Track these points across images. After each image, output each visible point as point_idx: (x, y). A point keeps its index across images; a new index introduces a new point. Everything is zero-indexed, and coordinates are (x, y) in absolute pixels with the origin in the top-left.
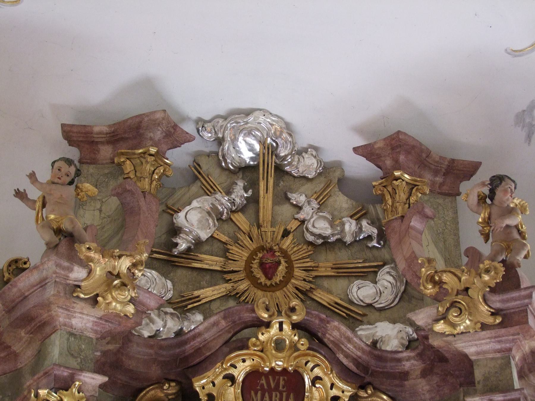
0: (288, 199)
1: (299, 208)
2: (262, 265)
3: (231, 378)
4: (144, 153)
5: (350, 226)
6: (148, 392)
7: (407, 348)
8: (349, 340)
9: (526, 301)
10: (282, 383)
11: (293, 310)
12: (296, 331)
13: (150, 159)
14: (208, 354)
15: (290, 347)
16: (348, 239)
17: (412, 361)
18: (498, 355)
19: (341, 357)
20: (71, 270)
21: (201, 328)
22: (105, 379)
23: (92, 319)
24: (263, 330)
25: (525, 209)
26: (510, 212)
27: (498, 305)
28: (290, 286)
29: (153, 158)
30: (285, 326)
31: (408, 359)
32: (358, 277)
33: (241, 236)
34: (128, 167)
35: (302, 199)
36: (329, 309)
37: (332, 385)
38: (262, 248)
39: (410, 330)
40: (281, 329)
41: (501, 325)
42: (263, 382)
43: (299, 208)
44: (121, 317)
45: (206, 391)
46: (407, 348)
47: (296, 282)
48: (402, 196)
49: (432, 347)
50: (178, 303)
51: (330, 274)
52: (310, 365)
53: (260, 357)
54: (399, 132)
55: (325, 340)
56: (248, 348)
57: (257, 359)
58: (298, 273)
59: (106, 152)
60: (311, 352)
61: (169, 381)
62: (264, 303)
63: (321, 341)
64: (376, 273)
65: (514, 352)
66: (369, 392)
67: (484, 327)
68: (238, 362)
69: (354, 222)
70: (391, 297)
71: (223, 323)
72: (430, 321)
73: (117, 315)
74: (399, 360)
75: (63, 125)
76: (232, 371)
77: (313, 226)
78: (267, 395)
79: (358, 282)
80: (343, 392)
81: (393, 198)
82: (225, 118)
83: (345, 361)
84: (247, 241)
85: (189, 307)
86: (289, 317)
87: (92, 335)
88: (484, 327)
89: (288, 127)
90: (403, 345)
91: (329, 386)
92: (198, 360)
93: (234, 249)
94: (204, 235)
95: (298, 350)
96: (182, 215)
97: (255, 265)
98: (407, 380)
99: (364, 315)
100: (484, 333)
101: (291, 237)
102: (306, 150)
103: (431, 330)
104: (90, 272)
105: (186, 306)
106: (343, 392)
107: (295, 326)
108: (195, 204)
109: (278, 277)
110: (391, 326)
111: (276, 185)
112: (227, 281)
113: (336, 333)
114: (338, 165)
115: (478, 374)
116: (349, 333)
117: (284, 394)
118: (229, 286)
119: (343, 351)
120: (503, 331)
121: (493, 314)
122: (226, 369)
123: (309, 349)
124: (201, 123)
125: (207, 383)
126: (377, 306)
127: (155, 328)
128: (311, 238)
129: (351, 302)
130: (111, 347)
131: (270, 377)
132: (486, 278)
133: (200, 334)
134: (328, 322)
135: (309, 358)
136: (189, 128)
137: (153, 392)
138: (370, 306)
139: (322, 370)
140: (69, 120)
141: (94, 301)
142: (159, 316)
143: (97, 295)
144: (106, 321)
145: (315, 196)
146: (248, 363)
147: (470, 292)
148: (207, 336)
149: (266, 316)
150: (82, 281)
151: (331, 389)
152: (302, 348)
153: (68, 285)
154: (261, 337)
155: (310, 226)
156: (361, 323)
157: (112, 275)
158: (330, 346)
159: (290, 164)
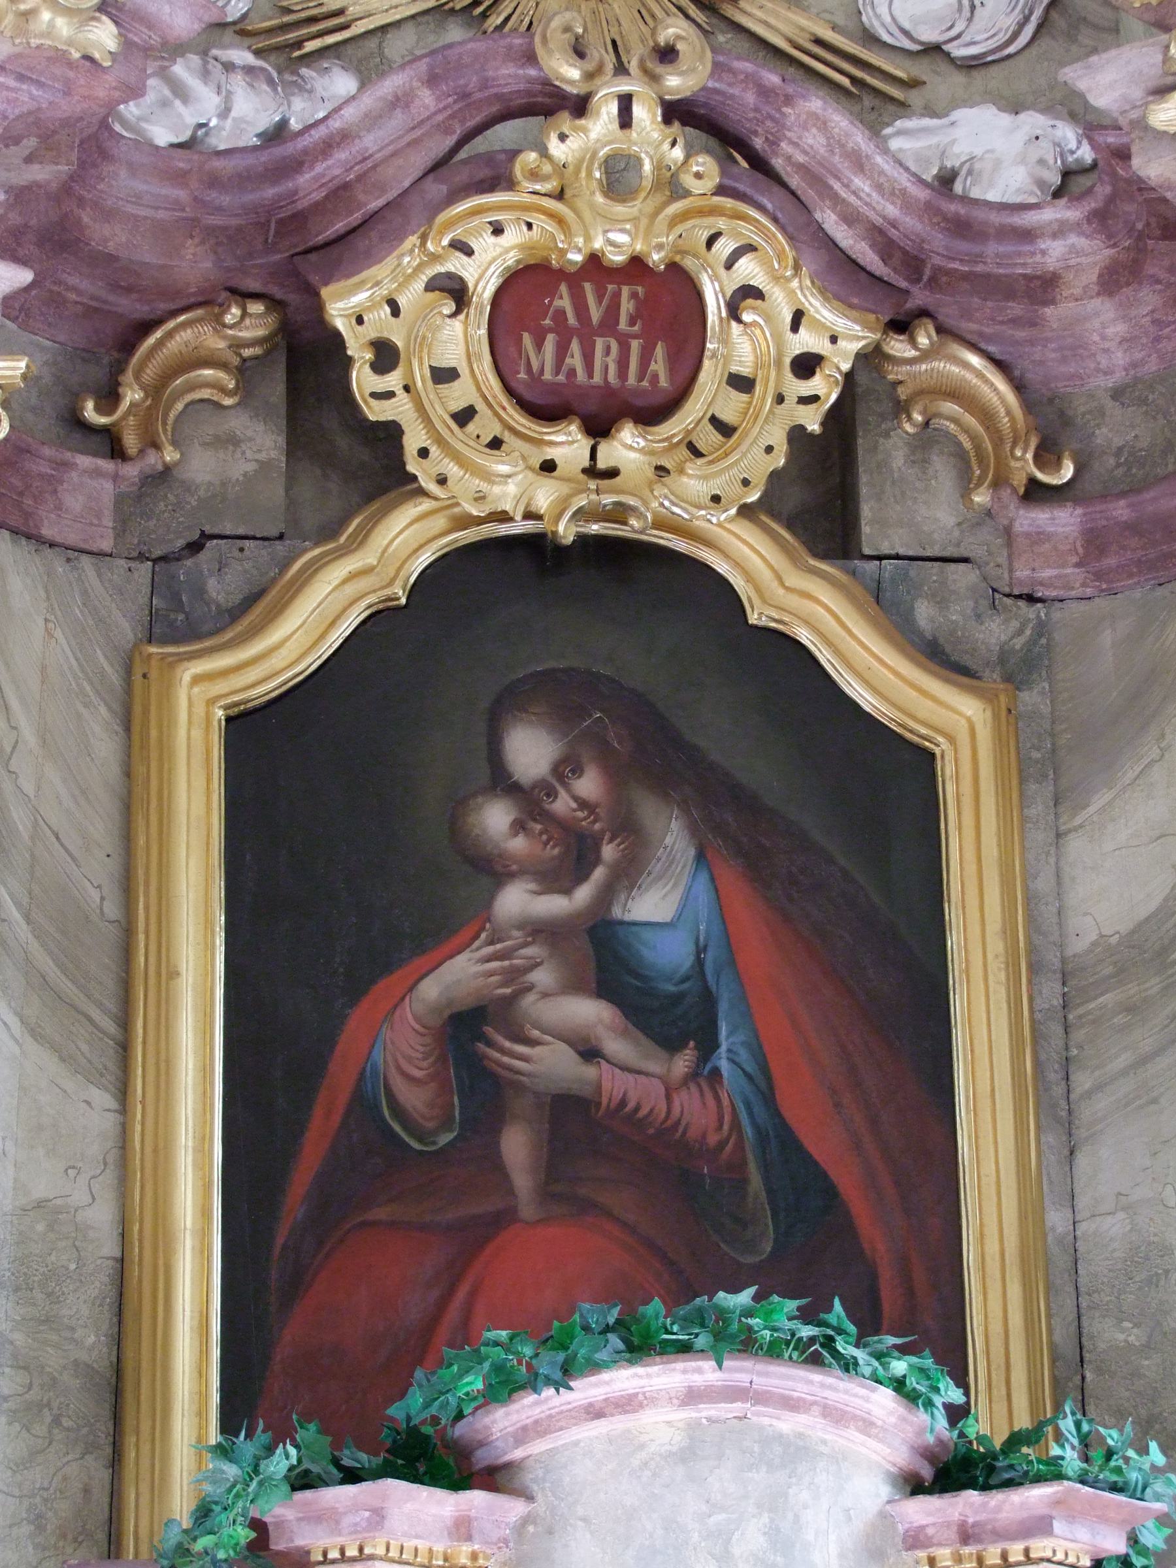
6: (170, 335)
7: (1057, 194)
8: (859, 163)
10: (627, 306)
11: (667, 54)
12: (677, 125)
14: (375, 204)
15: (657, 186)
17: (1073, 239)
19: (829, 220)
21: (350, 114)
22: (25, 276)
24: (565, 121)
31: (1060, 230)
36: (792, 60)
39: (1068, 134)
40: (625, 119)
42: (564, 302)
44: (70, 64)
45: (370, 331)
46: (1057, 194)
49: (1140, 186)
50: (270, 31)
52: (725, 247)
53: (551, 215)
55: (778, 163)
56: (510, 184)
57: (538, 220)
60: (728, 203)
62: (567, 29)
63: (759, 164)
66: (923, 341)
68: (478, 232)
70: (1009, 22)
71: (426, 99)
72: (1137, 93)
73: (59, 57)
74: (1027, 235)
76: (456, 264)
78: (575, 346)
80: (834, 339)
83: (844, 237)
85: (310, 46)
86: (653, 78)
90: (1041, 184)
91: (788, 318)
92: (340, 226)
98: (1053, 302)
99: (913, 84)
103: (1141, 124)
105: (299, 44)
106: (834, 339)
110: (1005, 119)
113: (814, 140)
116: (859, 139)
117: (635, 345)
119: (836, 201)
122: (435, 258)
123: (721, 190)
125: (373, 306)
126: (958, 51)
127: (189, 116)
129: (870, 39)
130: (39, 173)
131: (588, 287)
133: (344, 137)
134: (788, 100)
135: (721, 224)
137: (187, 335)
138: (934, 50)
139: (766, 264)
142: (205, 75)
144: (21, 78)
146: (513, 236)
148: (370, 142)
149: (574, 73)
151: (795, 327)
152: (697, 187)
158: (794, 181)
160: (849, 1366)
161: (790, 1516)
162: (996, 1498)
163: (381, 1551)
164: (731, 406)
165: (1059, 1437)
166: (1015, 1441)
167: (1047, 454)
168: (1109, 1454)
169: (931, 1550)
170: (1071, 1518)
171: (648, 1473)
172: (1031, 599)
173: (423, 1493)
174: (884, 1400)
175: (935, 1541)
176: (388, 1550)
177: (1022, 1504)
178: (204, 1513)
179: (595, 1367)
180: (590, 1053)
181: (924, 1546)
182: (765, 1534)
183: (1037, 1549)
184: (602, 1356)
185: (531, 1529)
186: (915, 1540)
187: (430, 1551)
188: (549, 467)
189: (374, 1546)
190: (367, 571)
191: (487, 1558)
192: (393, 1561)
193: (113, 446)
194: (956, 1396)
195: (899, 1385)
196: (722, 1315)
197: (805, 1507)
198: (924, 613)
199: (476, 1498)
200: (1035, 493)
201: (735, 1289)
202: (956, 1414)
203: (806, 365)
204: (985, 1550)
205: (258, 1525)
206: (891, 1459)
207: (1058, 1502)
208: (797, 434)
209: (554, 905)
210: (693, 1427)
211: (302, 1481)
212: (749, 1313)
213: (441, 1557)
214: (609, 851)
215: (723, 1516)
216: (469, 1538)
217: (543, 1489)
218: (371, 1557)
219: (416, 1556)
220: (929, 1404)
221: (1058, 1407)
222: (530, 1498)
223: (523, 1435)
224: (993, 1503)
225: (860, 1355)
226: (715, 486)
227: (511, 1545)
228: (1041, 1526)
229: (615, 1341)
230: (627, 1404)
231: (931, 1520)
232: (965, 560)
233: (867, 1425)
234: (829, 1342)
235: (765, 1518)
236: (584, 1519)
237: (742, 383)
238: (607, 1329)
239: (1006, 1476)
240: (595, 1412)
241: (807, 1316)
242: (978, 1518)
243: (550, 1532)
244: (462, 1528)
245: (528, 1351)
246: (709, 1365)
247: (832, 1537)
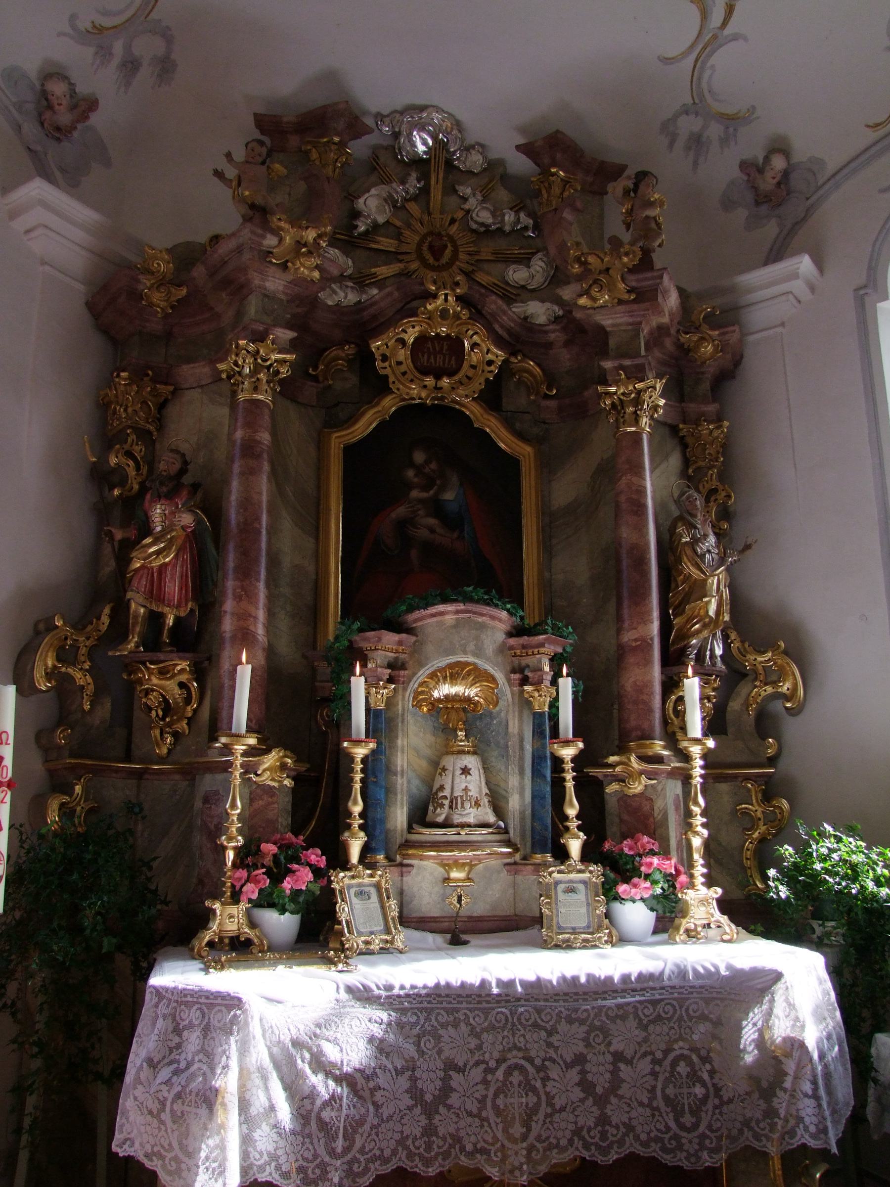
0: (456, 191)
1: (465, 199)
2: (431, 247)
3: (403, 342)
4: (328, 142)
5: (509, 217)
6: (331, 353)
7: (554, 322)
8: (505, 313)
9: (658, 281)
10: (445, 347)
11: (457, 284)
13: (334, 147)
14: (382, 320)
15: (454, 317)
16: (507, 228)
17: (557, 334)
18: (630, 327)
19: (497, 327)
20: (263, 237)
21: (377, 297)
22: (295, 334)
23: (283, 283)
24: (431, 301)
25: (663, 204)
26: (651, 204)
27: (634, 284)
28: (454, 267)
29: (336, 147)
30: (449, 298)
31: (554, 331)
32: (515, 262)
33: (413, 222)
34: (314, 155)
35: (469, 191)
37: (488, 351)
38: (431, 233)
39: (556, 308)
40: (446, 300)
41: (634, 301)
42: (430, 345)
43: (465, 199)
44: (308, 282)
45: (381, 352)
46: (554, 322)
47: (461, 265)
48: (556, 190)
49: (574, 319)
50: (357, 278)
51: (490, 258)
52: (470, 332)
53: (428, 324)
54: (557, 132)
55: (484, 312)
56: (417, 316)
57: (424, 325)
58: (462, 256)
59: (294, 141)
60: (471, 322)
61: (349, 343)
63: (479, 312)
64: (530, 259)
65: (643, 326)
67: (621, 302)
69: (513, 214)
70: (542, 280)
71: (396, 294)
72: (575, 296)
73: (305, 280)
74: (546, 332)
75: (255, 115)
76: (403, 335)
77: (477, 215)
78: (432, 357)
79: (513, 266)
81: (548, 192)
82: (402, 113)
84: (418, 226)
85: (367, 282)
86: (453, 290)
87: (282, 297)
88: (621, 302)
89: (458, 124)
90: (549, 320)
92: (374, 325)
93: (407, 233)
94: (381, 220)
95: (459, 318)
96: (361, 201)
97: (425, 247)
98: (551, 349)
100: (620, 307)
101: (457, 223)
102: (473, 147)
103: (576, 304)
104: (281, 240)
105: (364, 281)
107: (459, 299)
108: (373, 191)
109: (445, 259)
110: (540, 304)
111: (445, 178)
112: (401, 261)
113: (493, 306)
114: (500, 163)
115: (612, 342)
116: (505, 307)
118: (402, 266)
119: (498, 321)
120: (635, 306)
121: (628, 291)
122: (397, 334)
124: (380, 117)
126: (529, 287)
127: (336, 298)
128: (474, 226)
129: (507, 284)
130: (299, 310)
131: (436, 342)
132: (625, 260)
133: (375, 303)
134: (487, 296)
135: (470, 327)
136: (369, 122)
137: (335, 352)
138: (523, 287)
139: (480, 337)
140: (261, 110)
141: (284, 267)
142: (341, 288)
143: (287, 261)
144: (295, 285)
145: (480, 189)
146: (417, 329)
147: (611, 271)
148: (382, 304)
150: (274, 248)
152: (464, 317)
153: (261, 251)
154: (429, 307)
155: (474, 215)
156: (516, 301)
157: (300, 244)
158: (488, 317)
159: (458, 158)
160: (496, 606)
162: (532, 638)
164: (471, 373)
165: (547, 624)
166: (536, 625)
167: (550, 388)
168: (559, 628)
170: (549, 644)
172: (544, 423)
173: (391, 634)
174: (504, 614)
178: (337, 638)
179: (434, 605)
180: (432, 531)
184: (436, 602)
186: (511, 648)
188: (425, 387)
190: (379, 411)
193: (315, 379)
194: (522, 613)
195: (508, 610)
196: (465, 592)
198: (518, 425)
199: (404, 635)
200: (546, 397)
201: (469, 586)
202: (522, 618)
203: (490, 363)
205: (350, 641)
207: (546, 639)
208: (487, 380)
209: (424, 495)
210: (457, 619)
211: (361, 630)
212: (472, 592)
214: (438, 482)
220: (516, 615)
221: (546, 617)
223: (416, 621)
225: (499, 603)
226: (466, 392)
228: (542, 645)
229: (439, 598)
230: (442, 614)
232: (528, 413)
233: (500, 620)
234: (491, 600)
237: (474, 367)
238: (436, 596)
240: (433, 615)
241: (486, 593)
244: (400, 643)
245: (417, 600)
246: (462, 604)
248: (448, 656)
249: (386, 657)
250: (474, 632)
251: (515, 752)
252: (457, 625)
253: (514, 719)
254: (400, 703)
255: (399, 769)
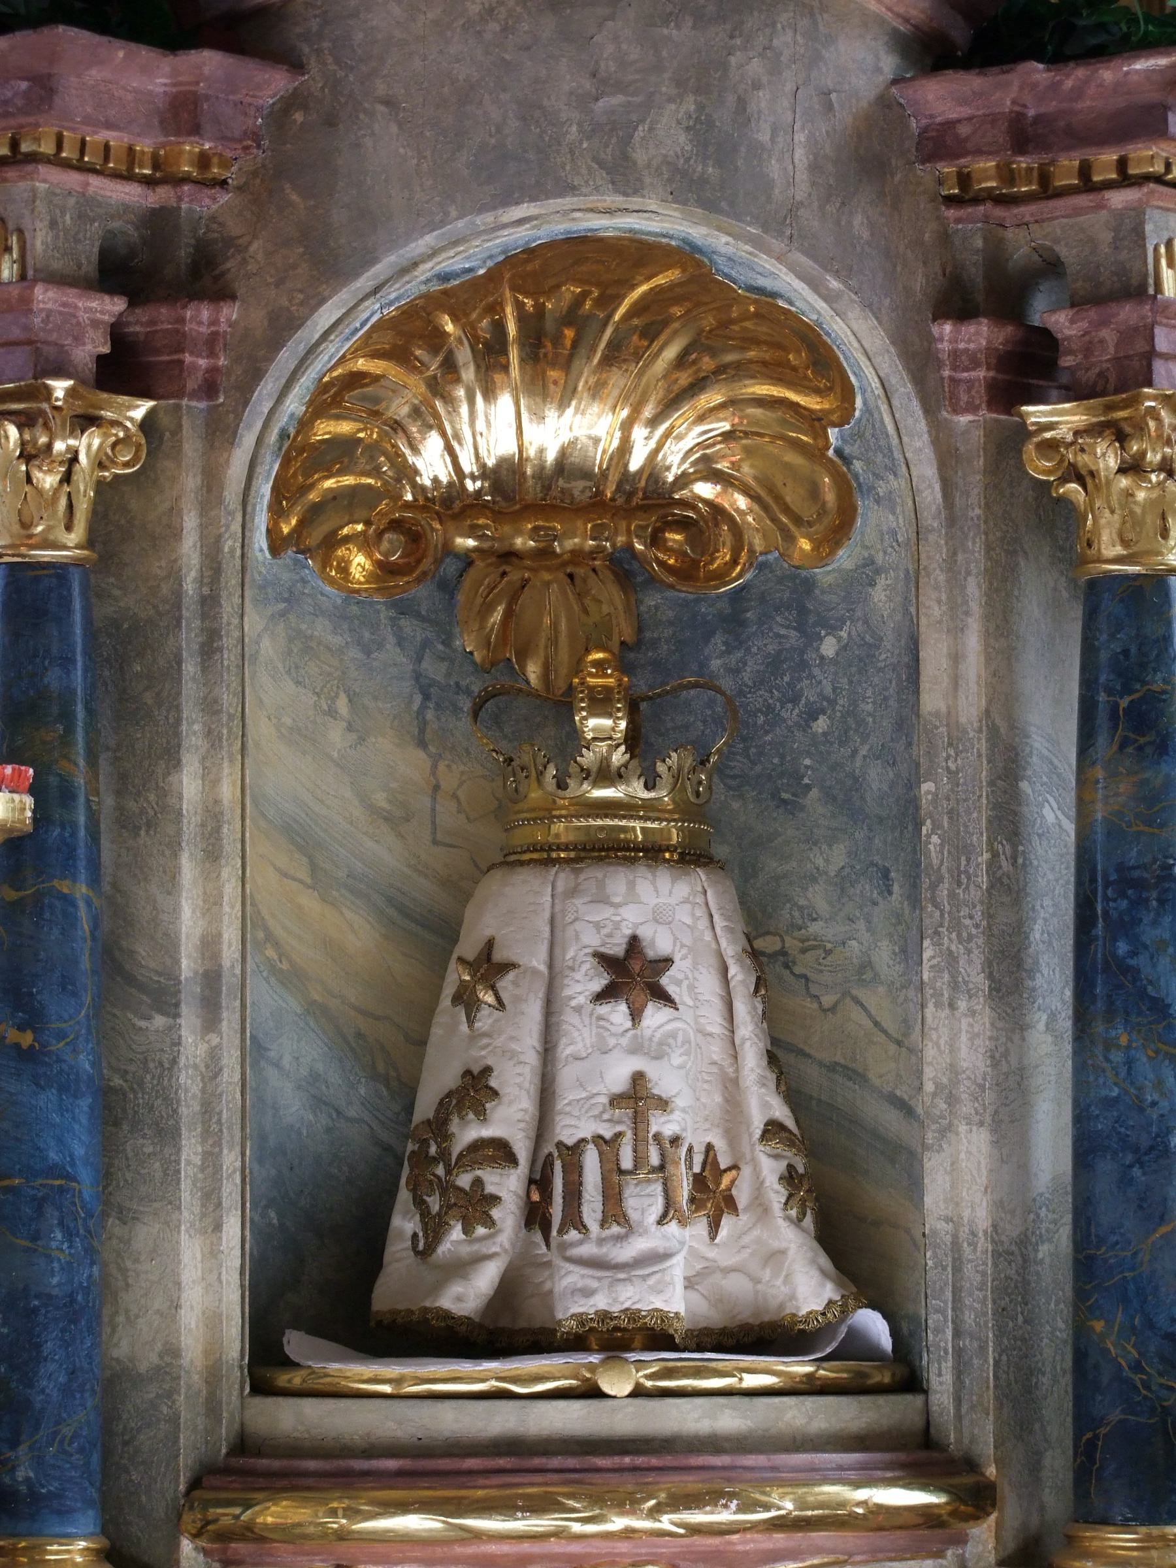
161: (731, 99)
162: (1075, 76)
163: (47, 148)
169: (962, 161)
171: (494, 26)
173: (120, 51)
175: (970, 146)
176: (59, 147)
177: (1117, 85)
181: (951, 154)
182: (688, 129)
183: (1140, 161)
185: (299, 117)
187: (131, 150)
189: (37, 140)
191: (225, 164)
192: (66, 165)
197: (757, 86)
204: (1053, 162)
206: (901, 10)
213: (148, 159)
215: (618, 100)
216: (195, 130)
217: (319, 52)
218: (34, 158)
219: (107, 159)
222: (297, 66)
224: (1069, 83)
227: (266, 143)
231: (965, 111)
235: (690, 105)
236: (388, 102)
239: (1093, 41)
242: (1042, 110)
243: (331, 121)
247: (800, 137)
248: (508, 199)
249: (87, 208)
250: (681, 34)
251: (960, 848)
252: (197, 83)
253: (957, 631)
254: (190, 522)
255: (188, 965)
